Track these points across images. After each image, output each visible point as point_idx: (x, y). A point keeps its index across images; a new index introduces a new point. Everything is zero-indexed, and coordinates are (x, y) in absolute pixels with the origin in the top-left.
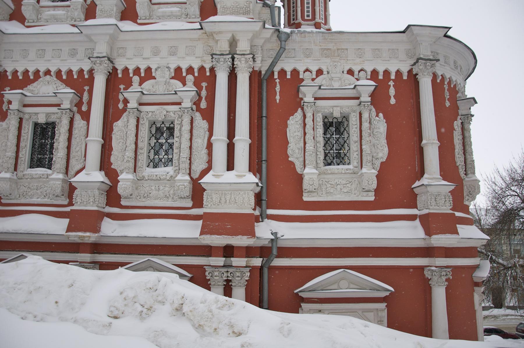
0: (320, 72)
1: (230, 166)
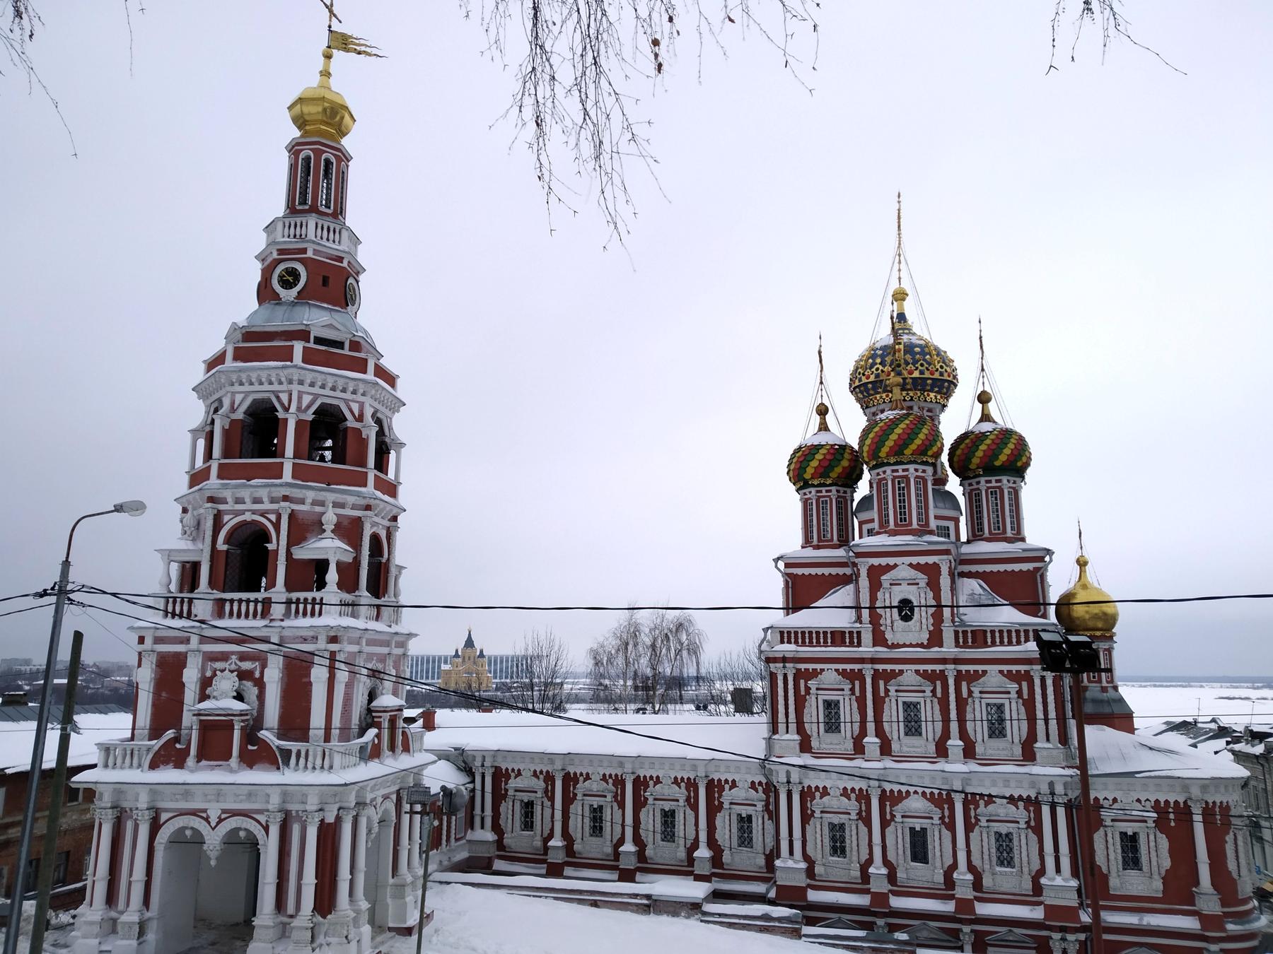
0: (1115, 800)
1: (1058, 870)
